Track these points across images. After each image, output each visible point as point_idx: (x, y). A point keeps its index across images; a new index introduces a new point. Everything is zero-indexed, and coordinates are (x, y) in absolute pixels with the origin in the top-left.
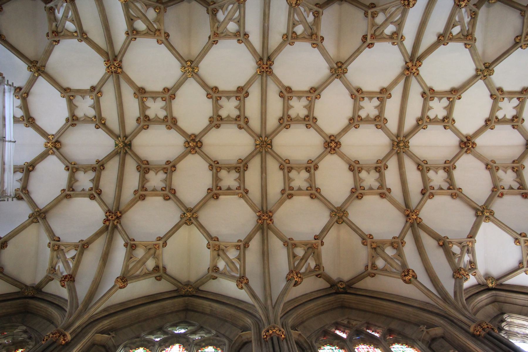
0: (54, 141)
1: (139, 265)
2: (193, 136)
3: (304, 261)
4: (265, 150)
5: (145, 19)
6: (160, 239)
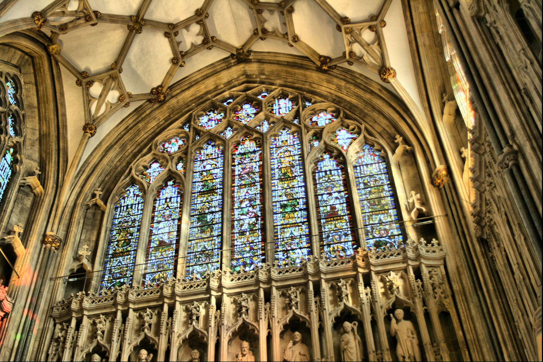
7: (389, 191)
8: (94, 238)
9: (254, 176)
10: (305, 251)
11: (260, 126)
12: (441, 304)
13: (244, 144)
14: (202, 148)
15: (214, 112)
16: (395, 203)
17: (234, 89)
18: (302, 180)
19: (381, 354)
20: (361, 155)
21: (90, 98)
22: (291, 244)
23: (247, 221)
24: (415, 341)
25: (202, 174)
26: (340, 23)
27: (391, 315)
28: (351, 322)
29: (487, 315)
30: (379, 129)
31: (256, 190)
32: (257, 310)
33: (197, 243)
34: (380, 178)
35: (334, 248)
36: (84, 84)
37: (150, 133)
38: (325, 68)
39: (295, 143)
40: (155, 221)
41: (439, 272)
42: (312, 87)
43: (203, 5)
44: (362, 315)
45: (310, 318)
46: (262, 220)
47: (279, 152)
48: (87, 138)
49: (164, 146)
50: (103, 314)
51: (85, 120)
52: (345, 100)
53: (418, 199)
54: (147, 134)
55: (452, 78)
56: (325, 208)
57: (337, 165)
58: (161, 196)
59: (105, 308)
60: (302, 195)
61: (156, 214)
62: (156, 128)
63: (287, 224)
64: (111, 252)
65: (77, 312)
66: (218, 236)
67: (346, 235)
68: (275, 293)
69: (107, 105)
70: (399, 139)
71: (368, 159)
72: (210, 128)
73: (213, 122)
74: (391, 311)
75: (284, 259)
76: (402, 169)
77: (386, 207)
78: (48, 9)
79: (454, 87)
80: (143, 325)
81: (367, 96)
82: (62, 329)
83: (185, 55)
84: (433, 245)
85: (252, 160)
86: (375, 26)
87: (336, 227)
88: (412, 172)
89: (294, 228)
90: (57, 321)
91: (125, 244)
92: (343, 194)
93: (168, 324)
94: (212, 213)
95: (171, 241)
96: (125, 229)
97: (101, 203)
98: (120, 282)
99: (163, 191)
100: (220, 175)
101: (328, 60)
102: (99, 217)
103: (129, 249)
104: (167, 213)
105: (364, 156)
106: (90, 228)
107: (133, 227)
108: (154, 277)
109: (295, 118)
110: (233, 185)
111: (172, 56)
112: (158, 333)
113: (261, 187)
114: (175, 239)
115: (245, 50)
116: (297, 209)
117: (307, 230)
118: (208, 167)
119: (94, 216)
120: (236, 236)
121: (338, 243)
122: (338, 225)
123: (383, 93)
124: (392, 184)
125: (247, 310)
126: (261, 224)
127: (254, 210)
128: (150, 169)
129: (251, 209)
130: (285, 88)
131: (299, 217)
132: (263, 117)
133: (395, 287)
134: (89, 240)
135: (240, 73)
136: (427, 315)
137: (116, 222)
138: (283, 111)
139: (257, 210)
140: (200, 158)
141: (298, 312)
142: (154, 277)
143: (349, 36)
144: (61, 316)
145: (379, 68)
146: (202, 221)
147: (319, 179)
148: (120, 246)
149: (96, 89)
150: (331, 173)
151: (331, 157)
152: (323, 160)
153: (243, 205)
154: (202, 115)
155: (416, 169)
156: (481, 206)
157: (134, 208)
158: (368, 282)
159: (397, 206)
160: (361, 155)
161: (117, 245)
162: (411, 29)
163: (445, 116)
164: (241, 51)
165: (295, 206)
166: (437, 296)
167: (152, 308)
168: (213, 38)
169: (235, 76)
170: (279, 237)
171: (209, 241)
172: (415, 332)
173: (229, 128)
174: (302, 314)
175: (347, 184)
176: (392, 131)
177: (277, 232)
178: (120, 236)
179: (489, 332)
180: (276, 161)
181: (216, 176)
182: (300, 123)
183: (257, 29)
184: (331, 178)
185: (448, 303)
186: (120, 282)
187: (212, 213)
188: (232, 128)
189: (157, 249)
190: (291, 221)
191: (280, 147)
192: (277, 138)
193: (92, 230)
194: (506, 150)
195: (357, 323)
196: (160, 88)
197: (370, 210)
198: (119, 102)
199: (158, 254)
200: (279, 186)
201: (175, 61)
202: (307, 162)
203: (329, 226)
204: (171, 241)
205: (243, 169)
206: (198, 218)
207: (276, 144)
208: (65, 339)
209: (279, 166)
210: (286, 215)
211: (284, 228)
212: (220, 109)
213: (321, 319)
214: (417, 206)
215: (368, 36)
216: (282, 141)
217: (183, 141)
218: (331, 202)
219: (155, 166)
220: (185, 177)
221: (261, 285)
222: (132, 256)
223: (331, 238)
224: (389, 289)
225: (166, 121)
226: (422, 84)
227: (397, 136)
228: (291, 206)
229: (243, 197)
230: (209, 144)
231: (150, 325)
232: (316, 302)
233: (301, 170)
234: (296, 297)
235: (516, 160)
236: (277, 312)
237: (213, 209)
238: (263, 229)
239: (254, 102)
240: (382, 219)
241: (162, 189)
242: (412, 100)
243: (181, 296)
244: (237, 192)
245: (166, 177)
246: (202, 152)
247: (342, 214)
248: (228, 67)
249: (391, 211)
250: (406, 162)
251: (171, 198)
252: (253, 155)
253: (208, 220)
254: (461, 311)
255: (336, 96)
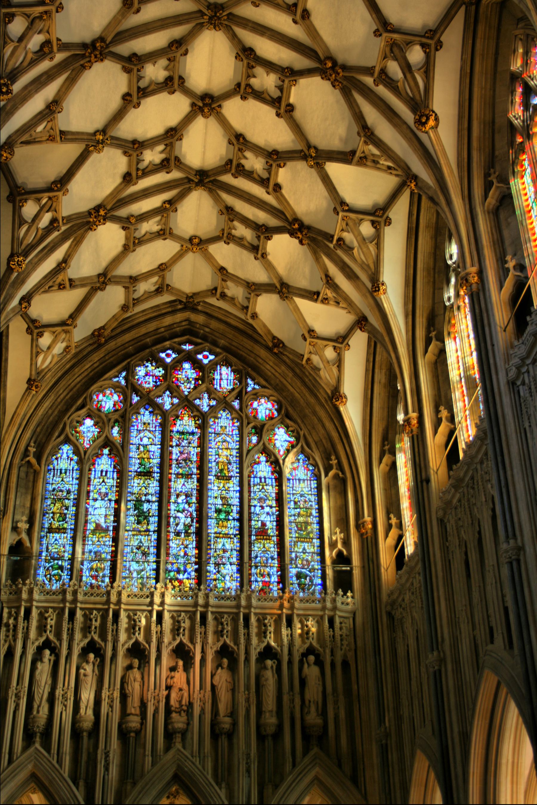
0: (189, 246)
1: (365, 250)
2: (194, 108)
3: (408, 76)
4: (224, 20)
5: (37, 217)
6: (335, 210)
7: (316, 517)
8: (28, 504)
9: (191, 466)
10: (234, 568)
11: (200, 399)
12: (345, 655)
13: (182, 419)
14: (139, 413)
15: (151, 364)
16: (320, 532)
17: (176, 340)
18: (237, 483)
19: (293, 695)
20: (295, 465)
21: (39, 350)
22: (222, 557)
23: (182, 521)
24: (321, 689)
25: (138, 449)
26: (307, 335)
27: (305, 659)
28: (271, 660)
29: (379, 680)
30: (316, 439)
31: (192, 485)
32: (192, 629)
33: (134, 535)
34: (309, 499)
35: (260, 570)
36: (35, 335)
37: (83, 375)
38: (276, 350)
39: (234, 433)
40: (91, 498)
41: (348, 625)
42: (257, 361)
43: (169, 261)
44: (282, 655)
45: (238, 649)
46: (197, 522)
47: (217, 440)
48: (31, 396)
49: (98, 397)
50: (52, 607)
51: (31, 375)
52: (289, 390)
53: (341, 539)
54: (80, 378)
55: (397, 436)
56: (256, 523)
57: (272, 473)
58: (96, 466)
59: (53, 602)
60: (236, 501)
61: (92, 488)
62: (89, 370)
63: (220, 533)
64: (46, 525)
65: (26, 601)
66: (154, 531)
67: (273, 558)
68: (210, 617)
69: (53, 357)
70: (334, 462)
71: (301, 473)
72: (147, 386)
73: (151, 377)
74: (305, 655)
75: (215, 574)
76: (331, 493)
77: (311, 535)
78: (34, 292)
79: (397, 446)
80: (90, 627)
81: (312, 400)
82: (10, 615)
83: (137, 301)
84: (348, 597)
85: (190, 443)
86: (340, 348)
87: (264, 547)
88: (340, 502)
89: (226, 540)
90: (4, 605)
91: (61, 519)
92: (274, 510)
93: (113, 631)
94: (148, 501)
95: (108, 527)
96: (60, 499)
97: (33, 461)
98: (57, 564)
99: (98, 460)
100: (158, 454)
101: (281, 345)
102: (31, 478)
103: (65, 526)
104: (103, 490)
105: (298, 467)
106: (24, 491)
107: (69, 500)
108: (92, 566)
109: (236, 398)
110: (171, 471)
111: (122, 302)
112: (104, 637)
113: (198, 482)
114: (112, 524)
115: (196, 301)
116: (231, 518)
117: (238, 545)
118: (145, 441)
119: (27, 476)
120: (172, 535)
121: (265, 566)
122: (266, 546)
123: (328, 405)
124: (320, 510)
125: (184, 630)
126: (196, 528)
127: (190, 509)
128: (83, 426)
129: (187, 506)
130: (229, 356)
131: (232, 527)
132: (205, 389)
133: (311, 633)
134: (24, 506)
135: (184, 318)
136: (333, 664)
137: (50, 488)
138: (224, 383)
139: (192, 509)
140: (138, 426)
141: (228, 641)
142: (92, 566)
143: (311, 347)
144: (9, 601)
145: (333, 389)
146: (138, 509)
147: (254, 485)
148: (56, 519)
149: (45, 340)
150: (265, 482)
151: (267, 461)
152: (259, 463)
153: (180, 500)
154: (139, 366)
155: (343, 500)
156: (398, 597)
157: (68, 474)
158: (290, 623)
159: (321, 537)
160: (295, 465)
161: (53, 518)
162: (371, 359)
163: (382, 465)
164: (191, 300)
165: (228, 513)
166: (343, 648)
167: (98, 610)
168: (168, 285)
169: (178, 321)
170: (212, 547)
171: (145, 535)
172: (321, 679)
173: (168, 393)
174: (232, 644)
175: (280, 499)
176: (328, 446)
177: (210, 541)
178: (56, 508)
179: (378, 694)
180: (214, 451)
181: (153, 455)
182: (241, 409)
183: (216, 289)
184: (265, 487)
185: (351, 655)
186: (57, 564)
187: (148, 501)
188: (171, 393)
189: (94, 532)
190: (225, 531)
191: (219, 434)
192: (216, 421)
193: (26, 493)
194: (435, 653)
195: (276, 662)
196: (102, 331)
197: (297, 535)
198: (65, 353)
199: (95, 539)
200: (216, 484)
201: (125, 308)
202: (245, 465)
203: (259, 545)
204: (108, 527)
205: (181, 453)
206: (135, 505)
207: (215, 429)
208: (15, 626)
209: (216, 459)
210: (220, 522)
211: (217, 537)
212: (159, 363)
213: (247, 653)
214: (340, 546)
215: (330, 353)
216: (221, 427)
217: (119, 396)
218: (262, 518)
219: (89, 422)
220: (122, 447)
221: (199, 608)
222: (69, 536)
223: (259, 558)
224: (306, 634)
225: (101, 364)
226: (368, 418)
227: (333, 457)
228: (225, 512)
229: (180, 490)
230: (147, 410)
231: (96, 628)
232: (244, 635)
233: (238, 470)
234: (227, 624)
235: (440, 666)
236: (210, 638)
237: (149, 497)
238: (199, 534)
239: (196, 365)
240: (306, 547)
241: (97, 457)
242: (355, 432)
243: (125, 604)
244: (174, 482)
245: (102, 444)
246: (139, 418)
247: (272, 534)
248: (173, 312)
249: (314, 541)
250: (335, 487)
251: (106, 472)
252: (191, 437)
253: (145, 510)
254: (359, 668)
255: (280, 381)
